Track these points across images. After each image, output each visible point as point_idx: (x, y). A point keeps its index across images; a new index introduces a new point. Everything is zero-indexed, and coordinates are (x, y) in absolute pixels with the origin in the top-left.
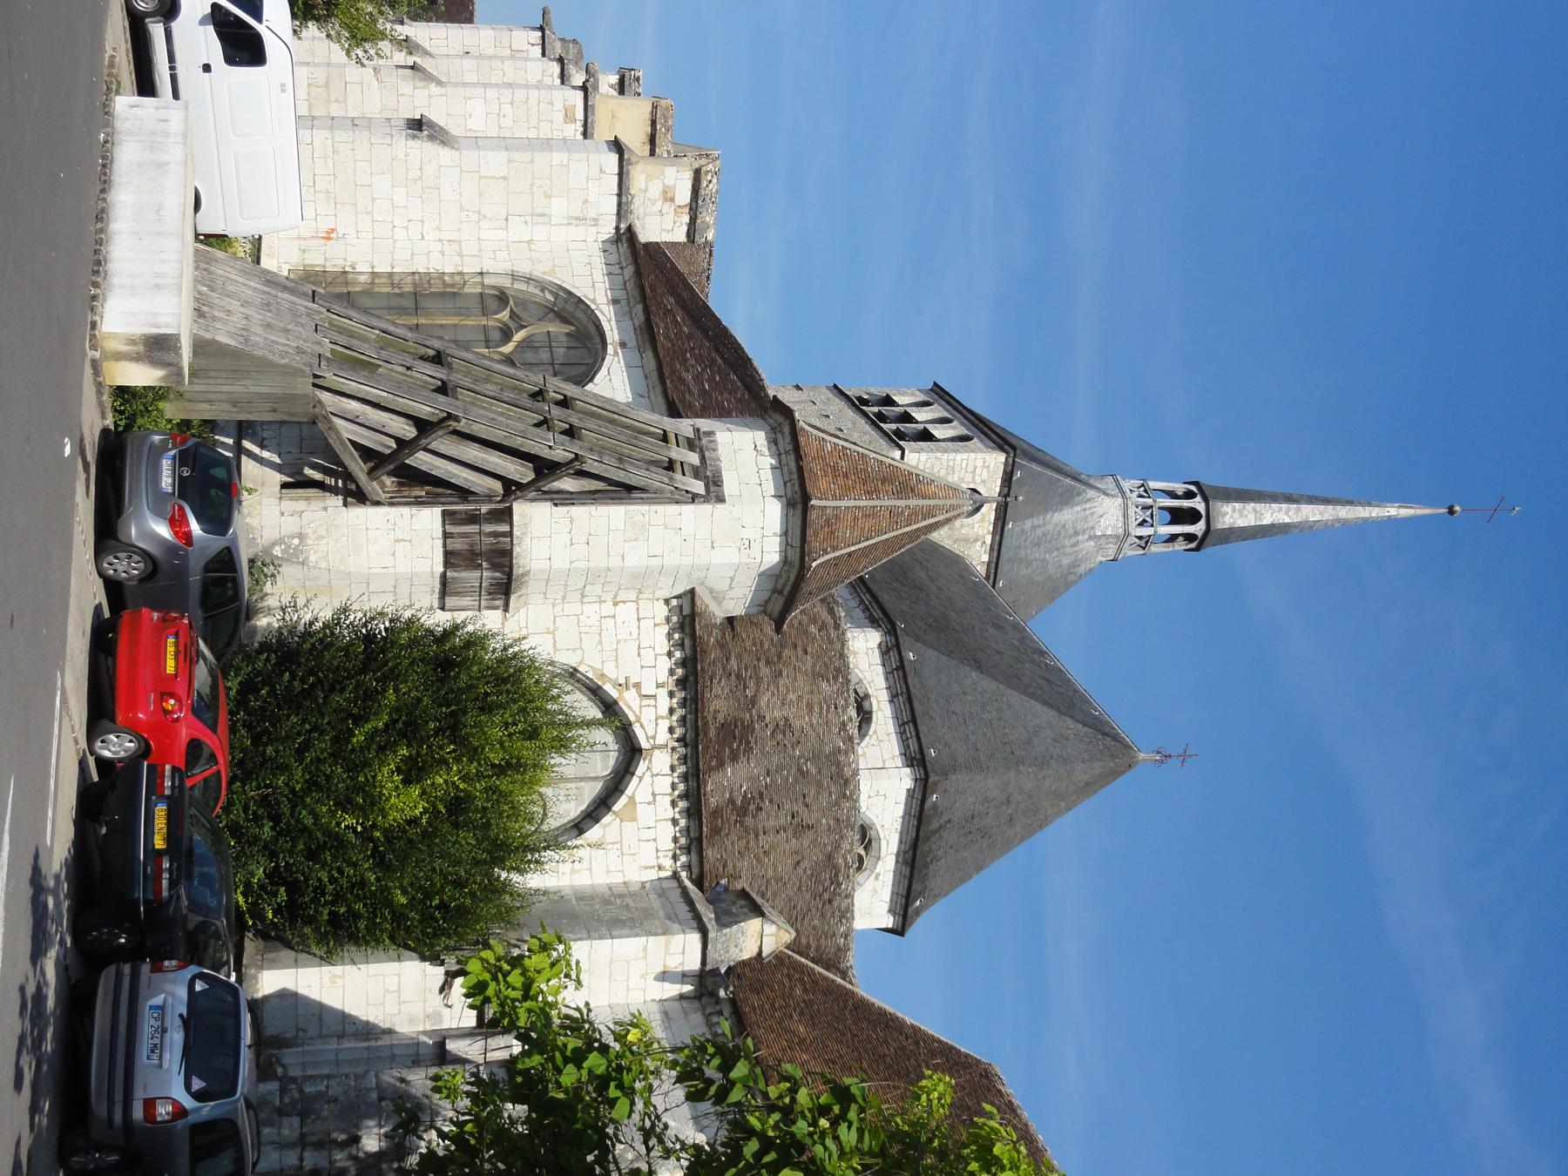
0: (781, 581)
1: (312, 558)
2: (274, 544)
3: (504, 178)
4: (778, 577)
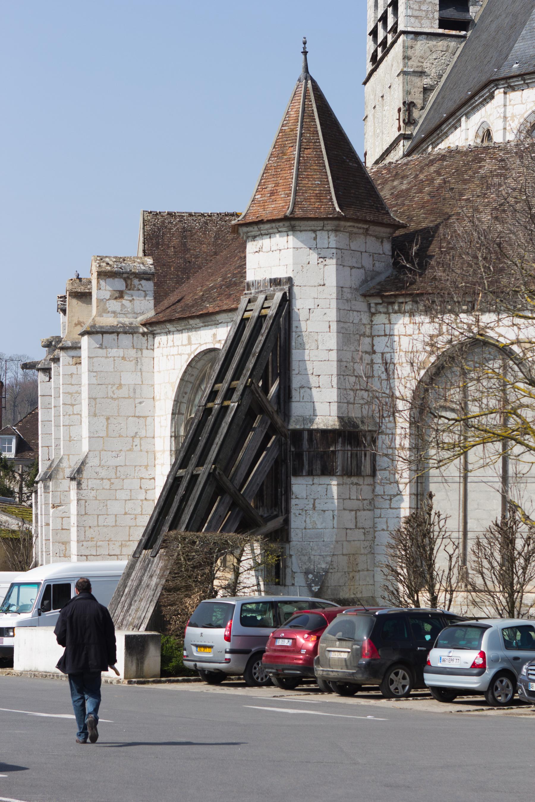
0: (355, 230)
1: (323, 566)
3: (108, 419)
4: (351, 233)
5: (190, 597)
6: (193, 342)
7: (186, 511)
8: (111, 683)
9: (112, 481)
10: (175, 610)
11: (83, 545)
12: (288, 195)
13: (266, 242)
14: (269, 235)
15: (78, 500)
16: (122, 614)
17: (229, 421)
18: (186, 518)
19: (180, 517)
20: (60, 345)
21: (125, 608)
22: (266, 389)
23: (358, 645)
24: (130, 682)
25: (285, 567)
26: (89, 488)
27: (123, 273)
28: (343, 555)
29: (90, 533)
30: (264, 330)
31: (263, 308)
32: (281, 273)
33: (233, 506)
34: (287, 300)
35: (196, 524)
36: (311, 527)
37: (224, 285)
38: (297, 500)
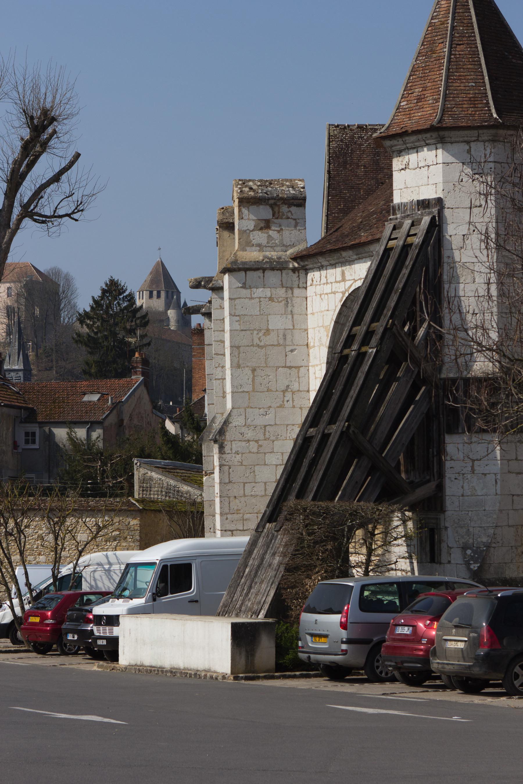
1: (485, 540)
2: (469, 569)
3: (254, 370)
5: (311, 578)
6: (347, 278)
7: (314, 477)
8: (216, 679)
9: (260, 443)
10: (297, 593)
11: (227, 519)
12: (437, 100)
13: (413, 158)
14: (416, 149)
15: (221, 466)
16: (241, 598)
17: (366, 370)
18: (314, 485)
19: (309, 484)
20: (210, 285)
21: (245, 592)
22: (414, 331)
23: (475, 632)
24: (236, 678)
25: (440, 541)
26: (234, 452)
27: (269, 199)
28: (509, 526)
29: (235, 504)
30: (409, 262)
31: (408, 235)
32: (429, 193)
33: (372, 470)
34: (437, 226)
35: (327, 492)
36: (469, 493)
37: (385, 210)
38: (452, 462)
